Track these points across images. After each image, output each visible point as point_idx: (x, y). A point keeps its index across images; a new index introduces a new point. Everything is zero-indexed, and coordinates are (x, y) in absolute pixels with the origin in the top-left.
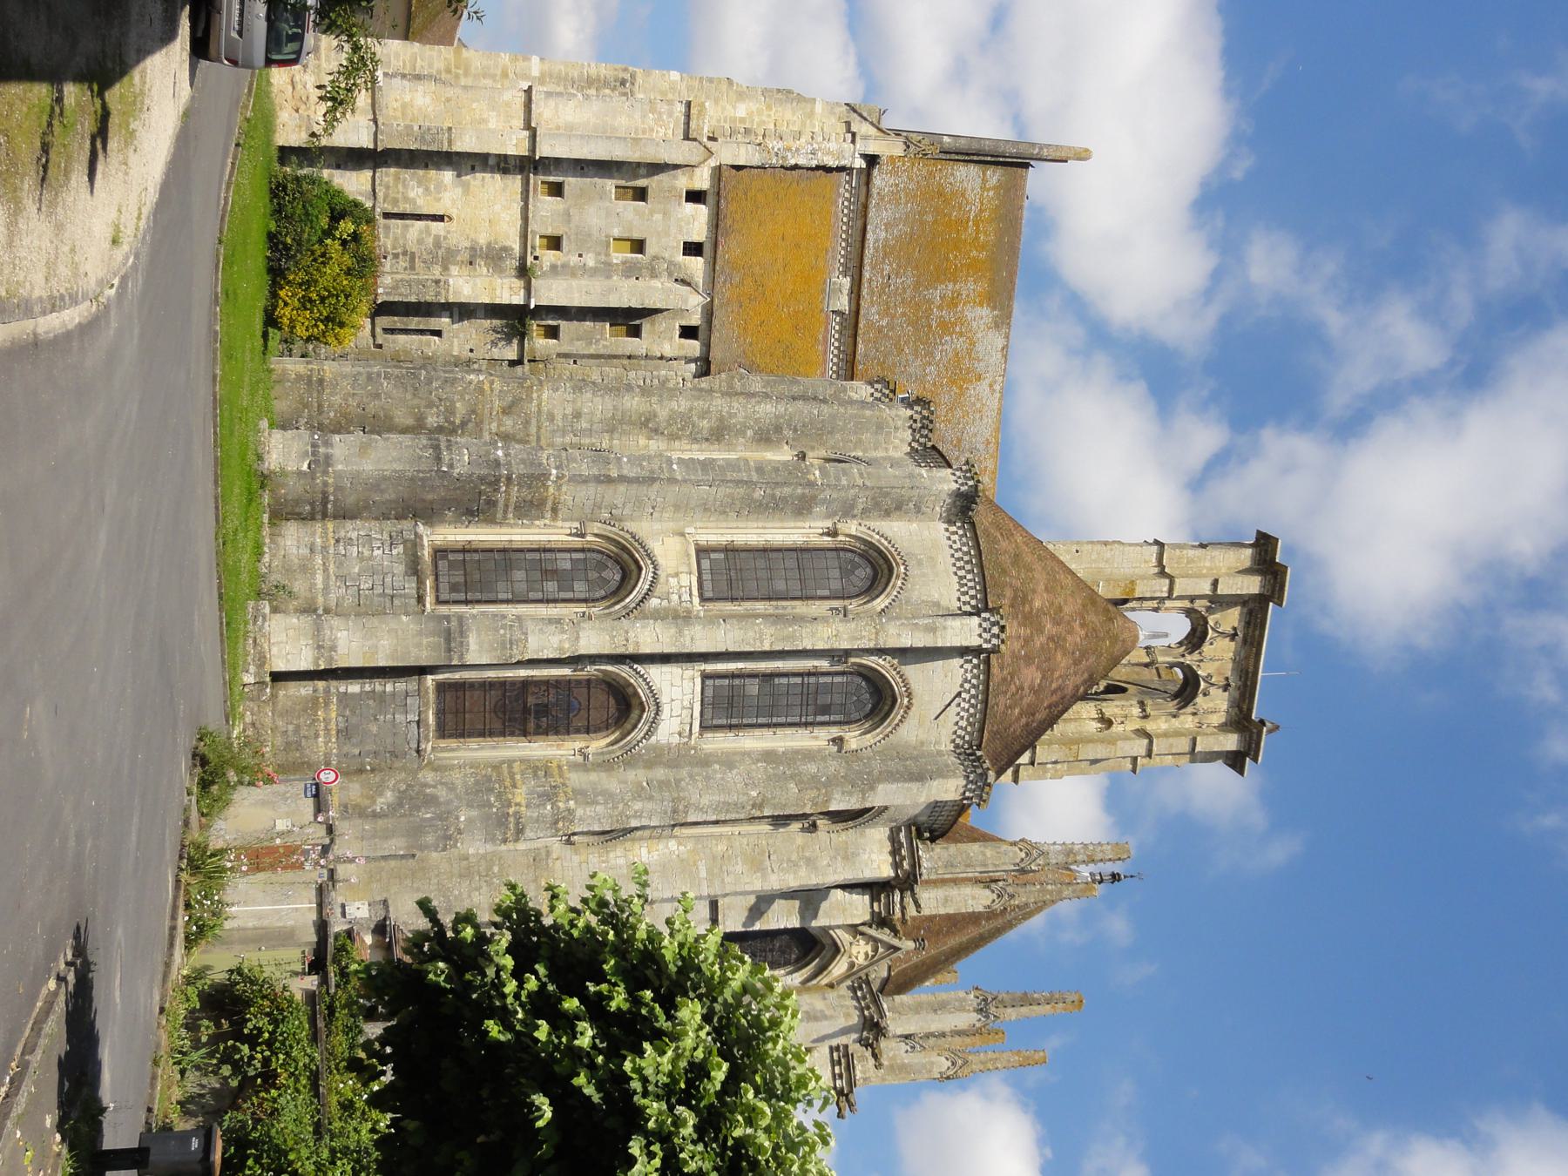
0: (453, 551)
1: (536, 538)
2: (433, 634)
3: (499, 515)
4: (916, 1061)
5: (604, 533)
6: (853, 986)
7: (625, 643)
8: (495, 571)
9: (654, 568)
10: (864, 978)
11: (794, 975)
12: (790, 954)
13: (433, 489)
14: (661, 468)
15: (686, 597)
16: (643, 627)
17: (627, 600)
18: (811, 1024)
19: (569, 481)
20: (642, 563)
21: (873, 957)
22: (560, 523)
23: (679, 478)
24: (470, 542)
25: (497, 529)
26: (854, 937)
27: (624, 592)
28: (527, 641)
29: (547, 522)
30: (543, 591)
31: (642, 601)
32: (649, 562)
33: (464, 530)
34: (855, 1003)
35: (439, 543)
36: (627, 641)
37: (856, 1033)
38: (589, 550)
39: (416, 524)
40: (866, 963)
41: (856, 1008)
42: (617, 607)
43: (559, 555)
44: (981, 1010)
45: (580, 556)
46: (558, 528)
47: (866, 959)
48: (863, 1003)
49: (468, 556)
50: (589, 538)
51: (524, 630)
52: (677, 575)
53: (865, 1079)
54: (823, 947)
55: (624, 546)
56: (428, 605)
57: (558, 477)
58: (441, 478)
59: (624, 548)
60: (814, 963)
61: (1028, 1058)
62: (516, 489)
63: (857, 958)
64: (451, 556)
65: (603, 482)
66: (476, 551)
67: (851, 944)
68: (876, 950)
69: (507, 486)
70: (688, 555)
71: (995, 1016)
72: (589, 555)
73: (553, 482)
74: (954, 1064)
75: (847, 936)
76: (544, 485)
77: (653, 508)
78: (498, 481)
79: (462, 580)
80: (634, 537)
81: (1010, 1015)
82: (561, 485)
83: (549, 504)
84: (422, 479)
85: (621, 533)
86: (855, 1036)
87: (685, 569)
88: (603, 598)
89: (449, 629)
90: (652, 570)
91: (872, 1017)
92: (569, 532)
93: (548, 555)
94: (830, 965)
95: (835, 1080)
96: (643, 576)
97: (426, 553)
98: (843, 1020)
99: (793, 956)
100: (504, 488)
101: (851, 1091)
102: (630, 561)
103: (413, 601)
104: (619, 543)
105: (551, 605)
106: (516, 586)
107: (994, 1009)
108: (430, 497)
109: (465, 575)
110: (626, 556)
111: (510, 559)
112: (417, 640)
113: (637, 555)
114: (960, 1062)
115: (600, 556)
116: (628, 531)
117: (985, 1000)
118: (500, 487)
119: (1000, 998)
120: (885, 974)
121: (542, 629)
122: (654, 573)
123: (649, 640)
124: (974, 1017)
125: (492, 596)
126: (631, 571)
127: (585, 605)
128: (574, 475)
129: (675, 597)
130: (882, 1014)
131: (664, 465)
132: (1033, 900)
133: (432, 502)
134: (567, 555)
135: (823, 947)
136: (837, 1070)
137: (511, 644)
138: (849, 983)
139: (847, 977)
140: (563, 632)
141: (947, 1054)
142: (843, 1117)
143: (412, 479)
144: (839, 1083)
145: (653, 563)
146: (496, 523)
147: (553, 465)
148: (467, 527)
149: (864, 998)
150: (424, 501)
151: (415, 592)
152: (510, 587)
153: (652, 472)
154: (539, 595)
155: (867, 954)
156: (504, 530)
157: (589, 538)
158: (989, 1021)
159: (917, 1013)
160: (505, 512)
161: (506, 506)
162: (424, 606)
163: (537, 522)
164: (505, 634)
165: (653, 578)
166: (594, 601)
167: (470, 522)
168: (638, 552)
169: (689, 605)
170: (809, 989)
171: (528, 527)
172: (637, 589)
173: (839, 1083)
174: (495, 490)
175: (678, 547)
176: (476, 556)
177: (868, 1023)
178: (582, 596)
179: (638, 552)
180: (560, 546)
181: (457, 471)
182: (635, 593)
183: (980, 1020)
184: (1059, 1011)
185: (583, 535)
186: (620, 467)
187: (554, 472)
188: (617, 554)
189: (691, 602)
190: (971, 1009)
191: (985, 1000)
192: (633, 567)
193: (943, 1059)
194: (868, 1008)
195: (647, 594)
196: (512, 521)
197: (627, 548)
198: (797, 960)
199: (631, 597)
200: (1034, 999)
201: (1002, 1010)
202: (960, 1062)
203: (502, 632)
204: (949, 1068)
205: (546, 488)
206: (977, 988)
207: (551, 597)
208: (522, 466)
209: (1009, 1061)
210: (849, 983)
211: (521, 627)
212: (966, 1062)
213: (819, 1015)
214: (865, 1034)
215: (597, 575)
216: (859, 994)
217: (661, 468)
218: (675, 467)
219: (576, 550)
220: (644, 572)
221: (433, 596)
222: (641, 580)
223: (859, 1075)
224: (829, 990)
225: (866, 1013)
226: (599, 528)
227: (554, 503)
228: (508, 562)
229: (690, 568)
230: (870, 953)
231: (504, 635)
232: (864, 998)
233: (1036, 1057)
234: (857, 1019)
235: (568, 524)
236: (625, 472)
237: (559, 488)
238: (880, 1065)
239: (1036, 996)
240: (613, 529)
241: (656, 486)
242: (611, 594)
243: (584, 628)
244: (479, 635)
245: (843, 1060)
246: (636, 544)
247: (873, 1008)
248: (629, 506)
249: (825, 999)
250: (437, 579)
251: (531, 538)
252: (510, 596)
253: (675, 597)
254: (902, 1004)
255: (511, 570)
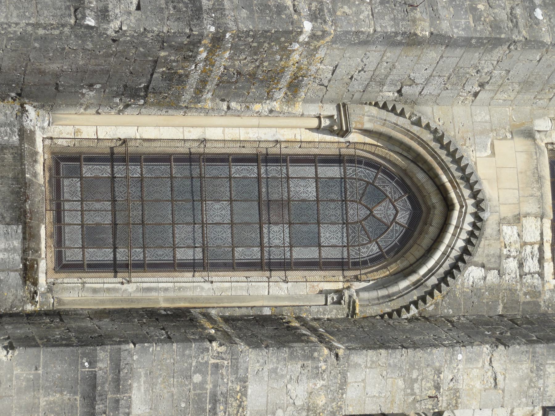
0: (92, 159)
1: (253, 134)
2: (60, 386)
3: (187, 97)
5: (384, 130)
7: (433, 392)
8: (172, 201)
9: (478, 205)
13: (62, 53)
14: (512, 16)
15: (532, 265)
16: (469, 360)
17: (423, 271)
19: (334, 41)
20: (453, 195)
22: (299, 108)
23: (547, 39)
24: (125, 141)
25: (177, 117)
27: (417, 252)
28: (245, 394)
29: (276, 105)
30: (261, 245)
31: (450, 273)
32: (467, 193)
33: (112, 117)
35: (64, 143)
36: (437, 387)
38: (353, 160)
39: (23, 110)
42: (404, 284)
43: (295, 170)
45: (334, 171)
46: (295, 116)
49: (120, 170)
50: (354, 137)
51: (241, 372)
52: (517, 219)
55: (418, 155)
56: (42, 279)
57: (313, 36)
58: (83, 38)
59: (417, 160)
62: (227, 55)
64: (88, 171)
65: (400, 44)
66: (136, 159)
69: (211, 52)
70: (540, 179)
72: (350, 170)
73: (301, 44)
76: (284, 49)
77: (482, 85)
78: (195, 43)
79: (108, 220)
80: (439, 139)
82: (316, 49)
83: (284, 82)
84: (43, 39)
85: (415, 129)
87: (531, 207)
88: (374, 260)
89: (94, 377)
90: (471, 209)
92: (314, 123)
93: (273, 170)
96: (454, 222)
97: (39, 168)
100: (204, 55)
102: (429, 187)
103: (15, 278)
104: (409, 149)
105: (277, 275)
106: (211, 232)
108: (55, 67)
109: (114, 213)
110: (421, 176)
111: (201, 177)
112: (27, 398)
113: (444, 179)
115: (372, 172)
116: (428, 126)
118: (198, 53)
121: (274, 371)
122: (477, 216)
123: (478, 385)
125: (164, 255)
126: (430, 209)
127: (338, 274)
128: (347, 32)
129: (511, 265)
131: (518, 11)
133: (57, 75)
134: (309, 171)
137: (214, 401)
140: (317, 374)
143: (22, 38)
145: (474, 195)
146: (178, 107)
147: (305, 11)
148: (120, 112)
150: (42, 73)
151: (17, 258)
152: (198, 235)
153: (496, 26)
154: (255, 253)
156: (193, 118)
157: (354, 137)
160: (199, 91)
161: (203, 82)
162: (35, 283)
163: (257, 107)
164: (204, 382)
165: (474, 225)
166: (356, 265)
167: (127, 106)
168: (446, 170)
169: (536, 281)
171: (238, 115)
172: (442, 248)
174: (185, 59)
175: (521, 161)
176: (135, 171)
178: (334, 254)
179: (446, 170)
180: (296, 150)
181: (115, 25)
182: (438, 255)
185: (343, 133)
186: (435, 17)
187: (308, 26)
188: (405, 171)
189: (541, 275)
192: (435, 199)
195: (460, 258)
196: (209, 105)
197: (425, 161)
199: (431, 263)
203: (197, 378)
205: (286, 53)
207: (277, 255)
208: (244, 13)
211: (235, 367)
215: (364, 212)
217: (512, 16)
218: (539, 13)
219: (327, 160)
220: (456, 214)
221: (51, 255)
222: (451, 230)
226: (372, 119)
227: (295, 77)
228: (197, 183)
229: (542, 207)
231: (201, 385)
235: (314, 109)
236: (445, 26)
237: (311, 53)
240: (401, 121)
241: (499, 53)
242: (388, 252)
243: (357, 365)
244: (152, 385)
246: (443, 154)
248: (437, 81)
250: (58, 219)
251: (243, 134)
252: (199, 255)
253: (511, 265)
255: (202, 200)
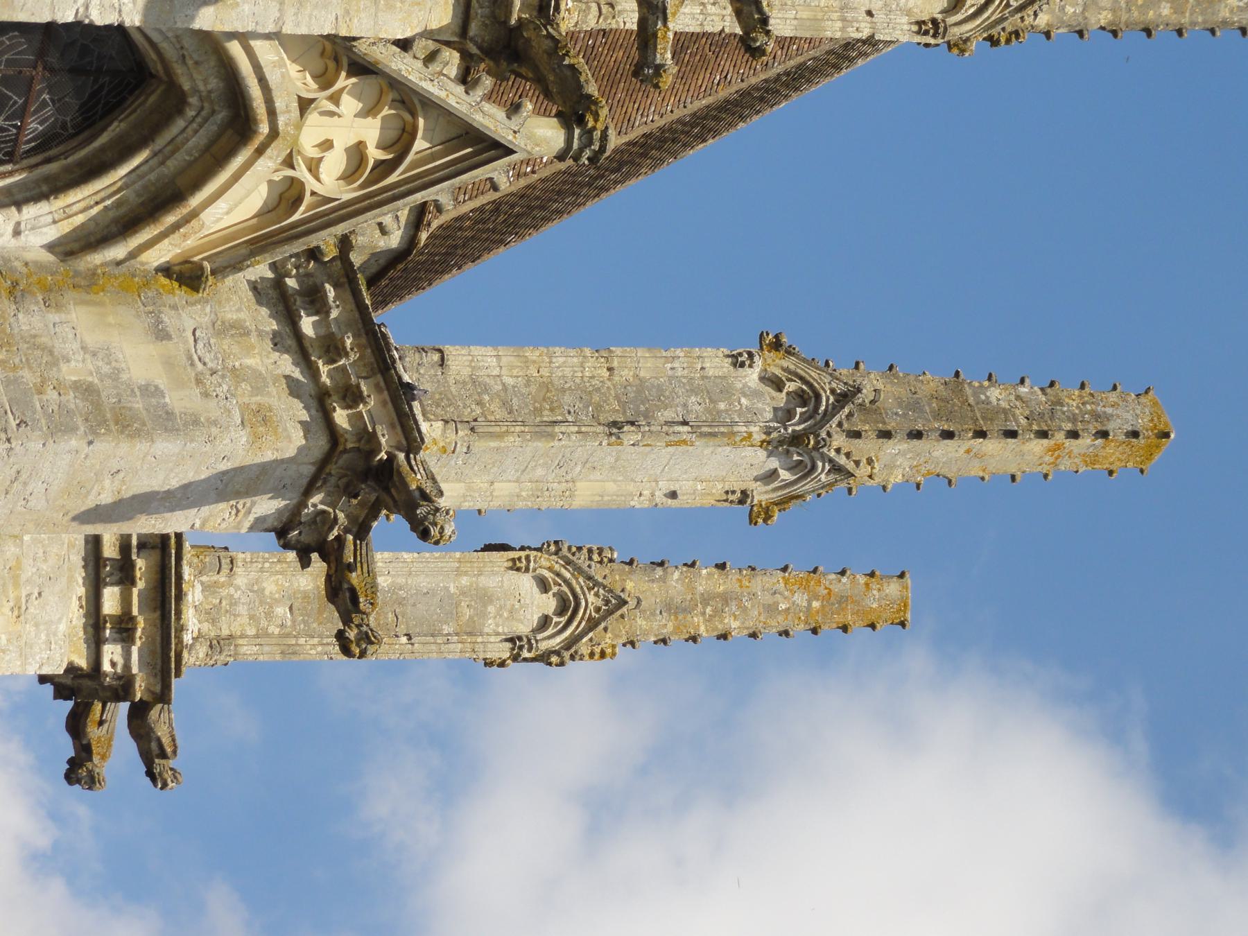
4: (423, 582)
6: (278, 283)
10: (330, 252)
11: (30, 211)
12: (22, 113)
18: (103, 446)
21: (383, 168)
26: (325, 80)
34: (287, 365)
37: (277, 493)
40: (347, 194)
41: (294, 388)
44: (796, 440)
47: (348, 177)
48: (324, 369)
53: (217, 644)
54: (175, 102)
60: (123, 170)
61: (843, 600)
63: (314, 167)
67: (305, 105)
68: (399, 143)
71: (836, 469)
74: (567, 606)
75: (293, 69)
81: (890, 467)
86: (268, 506)
91: (368, 440)
94: (197, 185)
95: (96, 642)
98: (243, 437)
99: (34, 126)
101: (163, 696)
107: (839, 440)
114: (592, 600)
117: (807, 397)
119: (867, 394)
120: (394, 240)
124: (761, 460)
130: (412, 442)
132: (1104, 18)
135: (175, 102)
136: (111, 601)
138: (261, 270)
139: (258, 246)
141: (544, 564)
142: (92, 782)
144: (111, 653)
149: (332, 349)
155: (357, 152)
158: (807, 486)
159: (546, 429)
170: (91, 283)
173: (111, 653)
177: (343, 460)
183: (772, 475)
184: (1065, 465)
190: (758, 437)
191: (807, 397)
193: (526, 583)
194: (352, 397)
198: (45, 143)
200: (994, 412)
201: (867, 446)
202: (592, 600)
204: (545, 622)
206: (777, 345)
209: (771, 609)
210: (261, 270)
212: (616, 604)
213: (138, 404)
214: (317, 500)
216: (308, 325)
223: (192, 622)
224: (181, 295)
225: (341, 417)
230: (374, 154)
232: (332, 349)
233: (873, 602)
234: (297, 439)
238: (367, 638)
239: (995, 394)
245: (140, 564)
247: (372, 404)
249: (161, 334)
254: (476, 385)
